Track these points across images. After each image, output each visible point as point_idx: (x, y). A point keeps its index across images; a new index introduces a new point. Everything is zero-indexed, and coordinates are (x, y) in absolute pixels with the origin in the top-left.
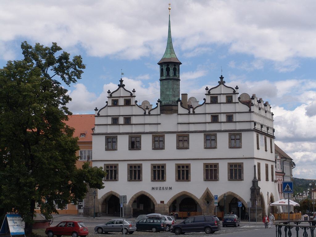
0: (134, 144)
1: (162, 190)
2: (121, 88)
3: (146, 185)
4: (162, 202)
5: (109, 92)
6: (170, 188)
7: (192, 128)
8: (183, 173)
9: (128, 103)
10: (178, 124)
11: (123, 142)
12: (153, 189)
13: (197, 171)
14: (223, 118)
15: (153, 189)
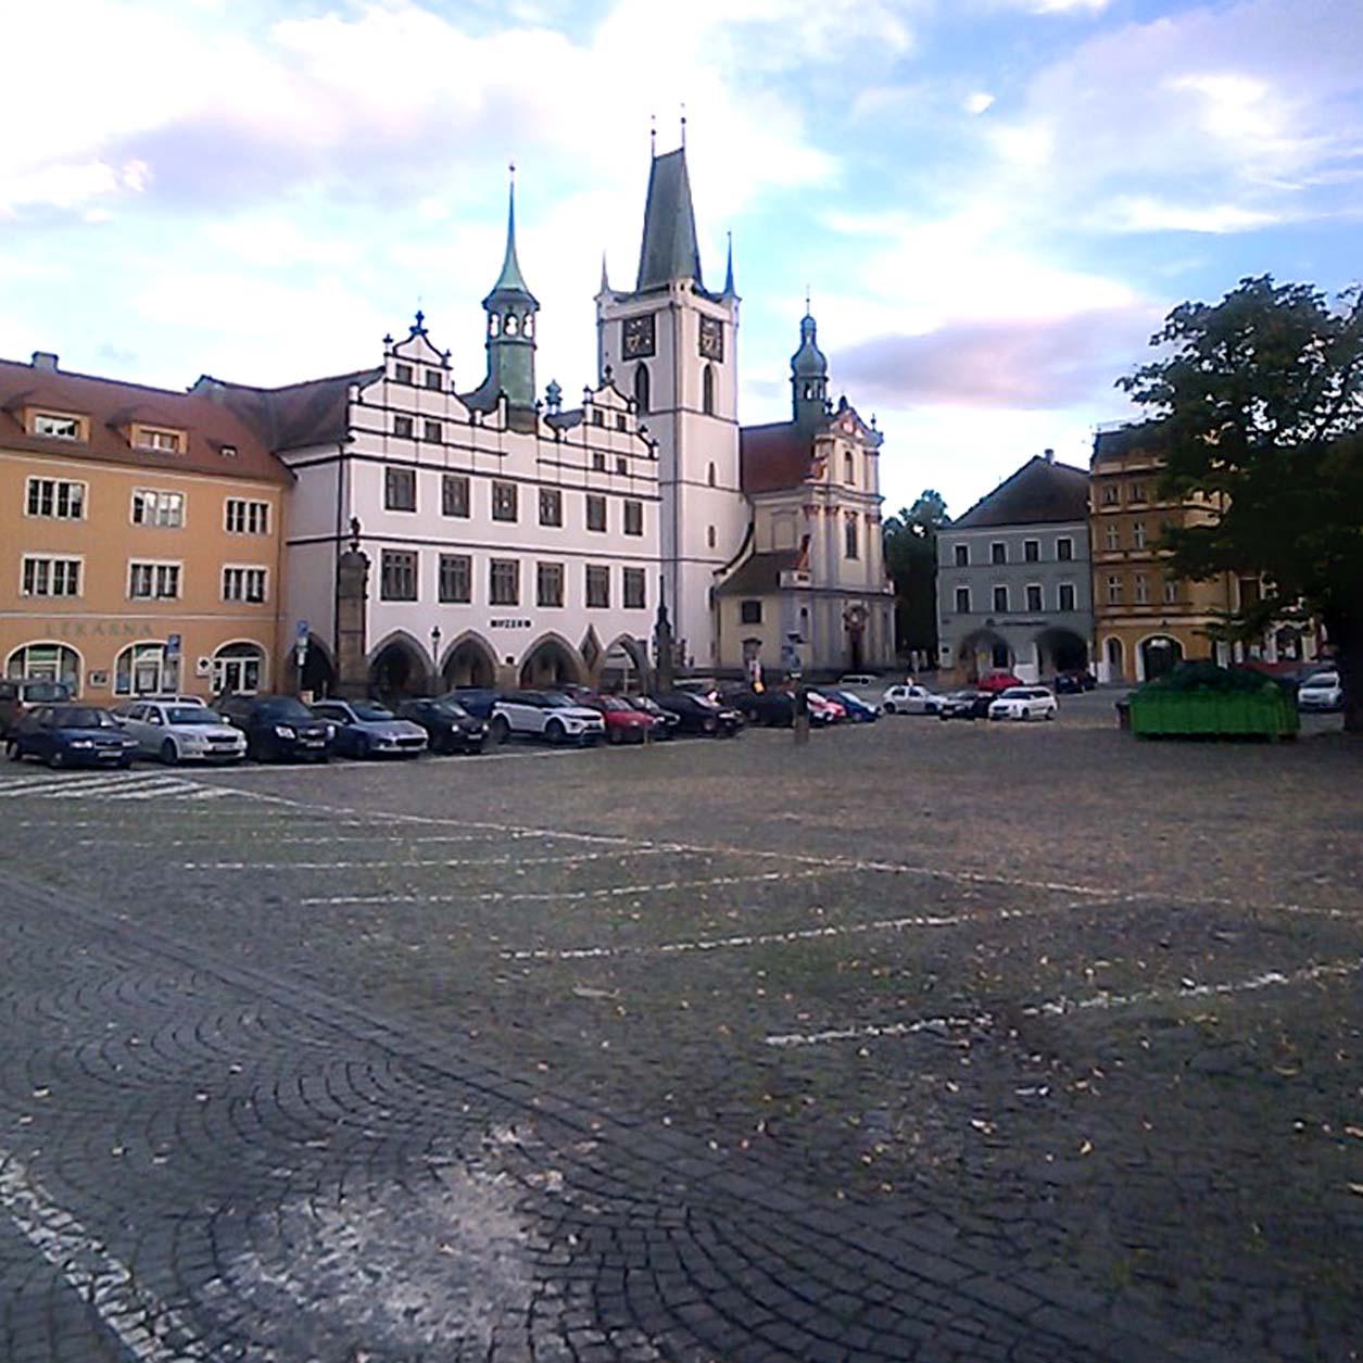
0: (456, 501)
1: (517, 629)
2: (419, 338)
3: (476, 615)
4: (510, 660)
5: (388, 340)
6: (528, 624)
7: (567, 476)
8: (550, 588)
9: (434, 383)
10: (539, 461)
11: (429, 488)
12: (494, 624)
13: (575, 585)
14: (611, 463)
15: (494, 624)
